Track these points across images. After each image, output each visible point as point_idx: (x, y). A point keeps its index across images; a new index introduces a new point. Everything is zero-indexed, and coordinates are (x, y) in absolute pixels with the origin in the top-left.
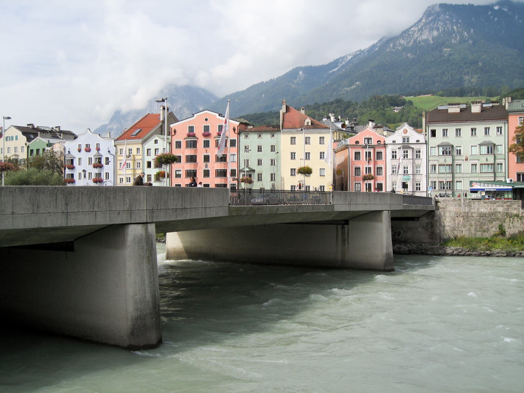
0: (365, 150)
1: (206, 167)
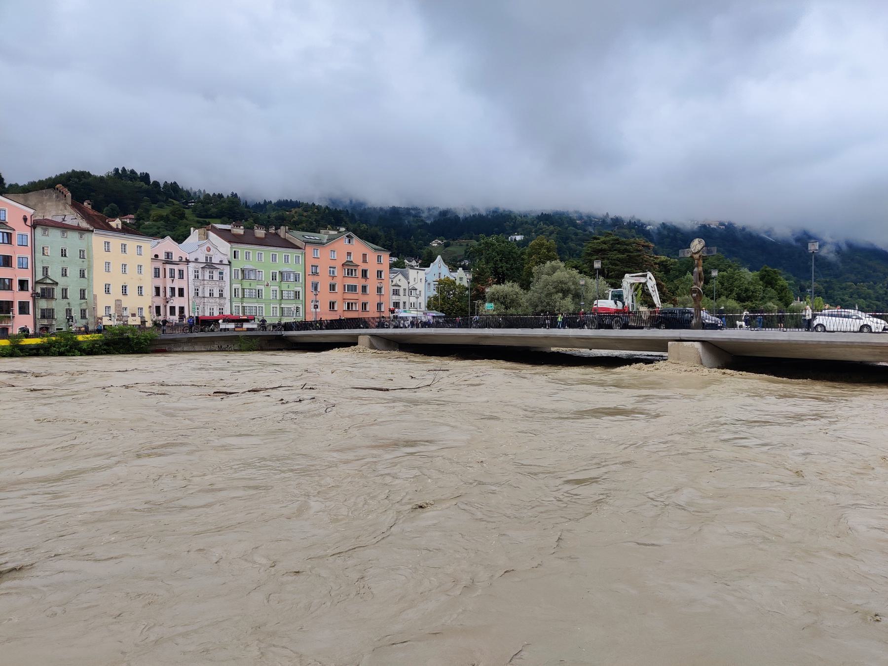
0: (168, 267)
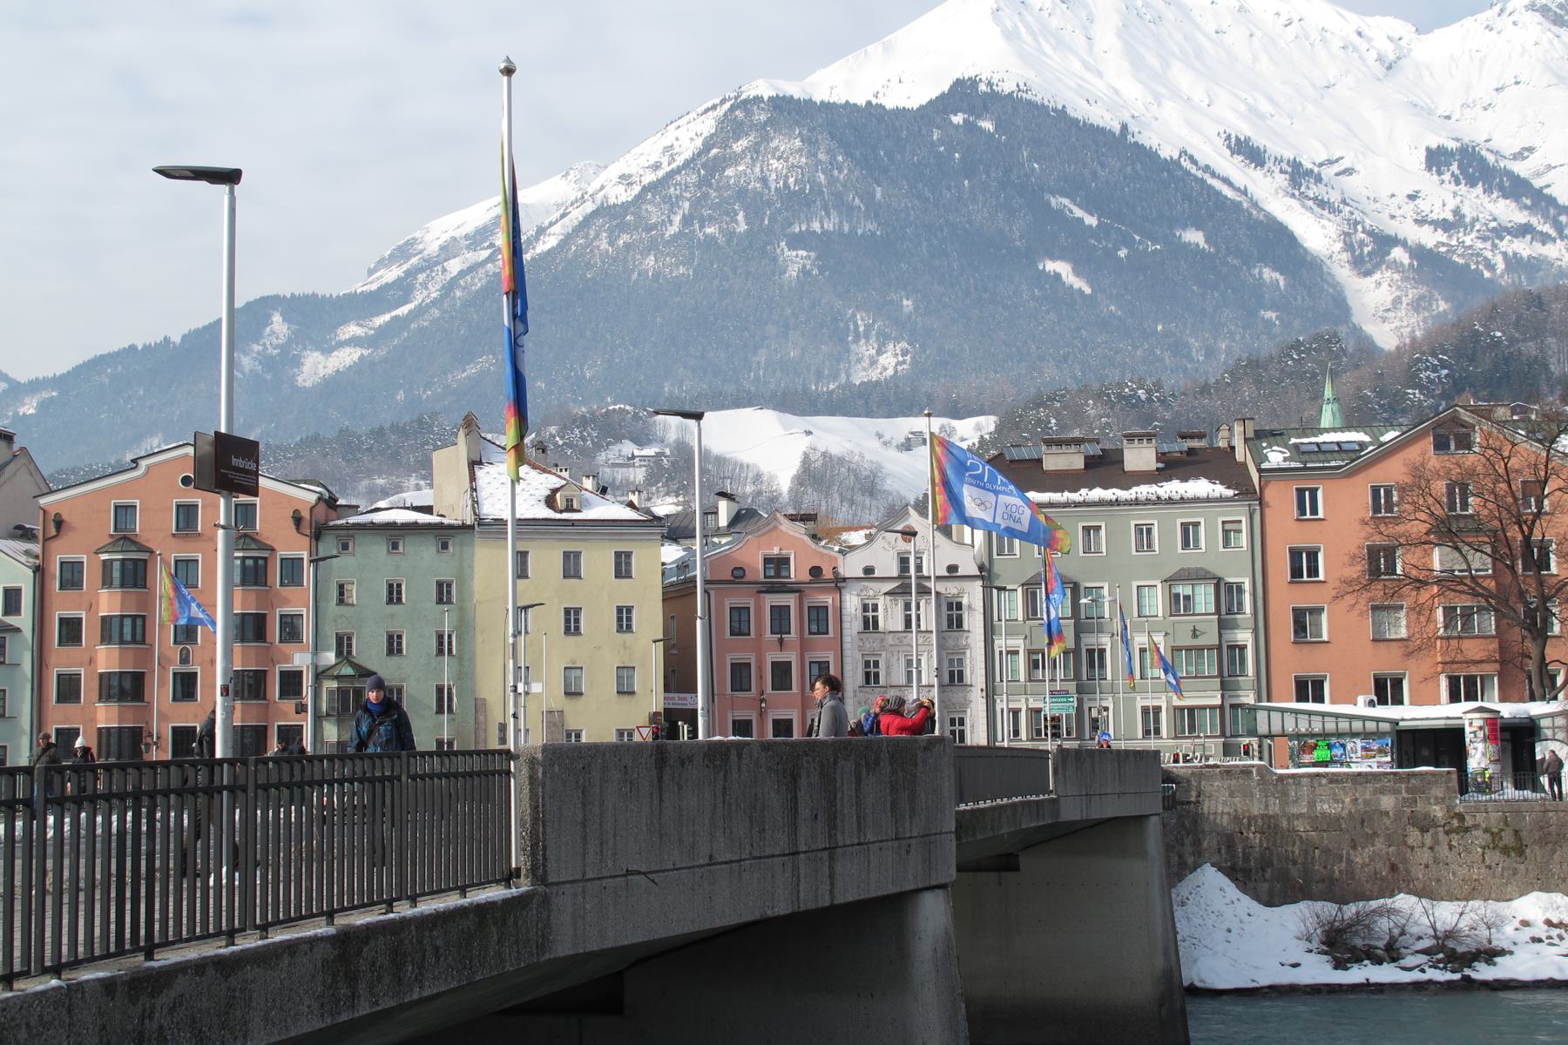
0: (771, 600)
1: (185, 660)
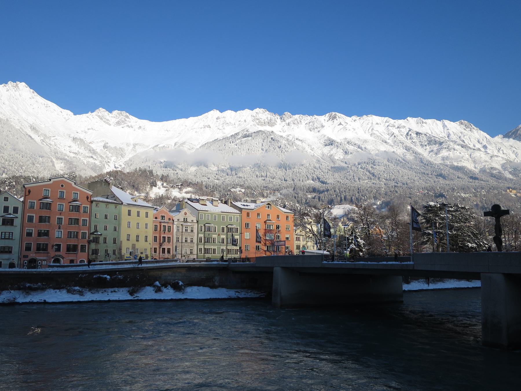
0: (163, 224)
